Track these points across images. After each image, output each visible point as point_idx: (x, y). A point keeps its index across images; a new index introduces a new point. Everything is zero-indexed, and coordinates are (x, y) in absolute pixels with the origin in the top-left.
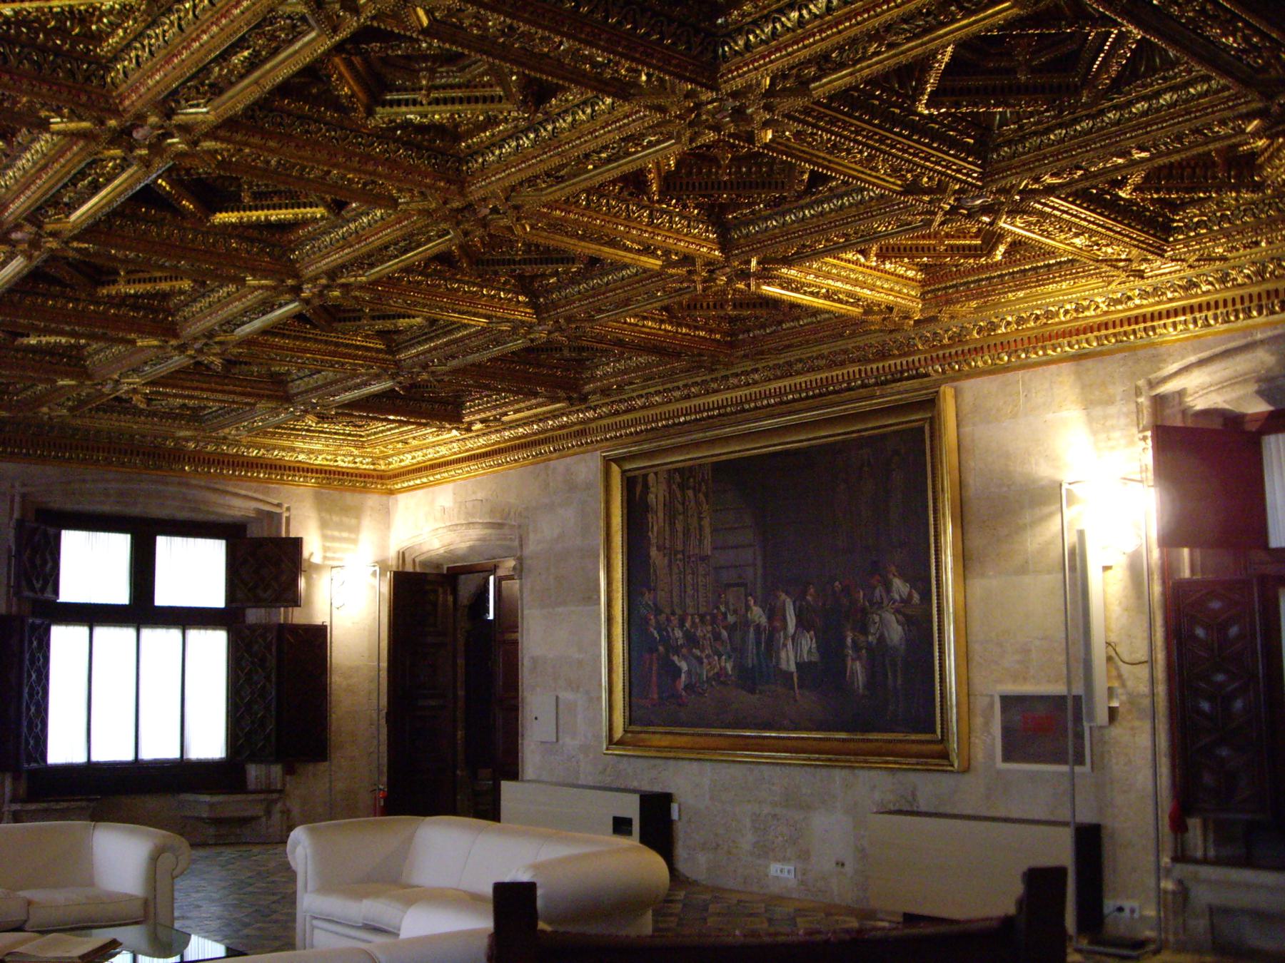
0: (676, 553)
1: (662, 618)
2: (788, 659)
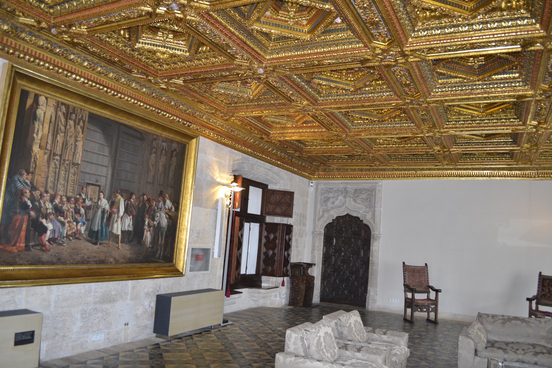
0: (55, 155)
1: (37, 194)
2: (117, 228)
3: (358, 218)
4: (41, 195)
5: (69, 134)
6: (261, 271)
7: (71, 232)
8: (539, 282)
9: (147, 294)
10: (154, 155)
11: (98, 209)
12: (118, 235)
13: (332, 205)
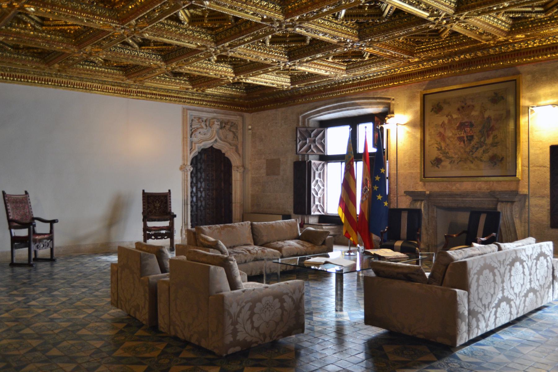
8: (143, 199)
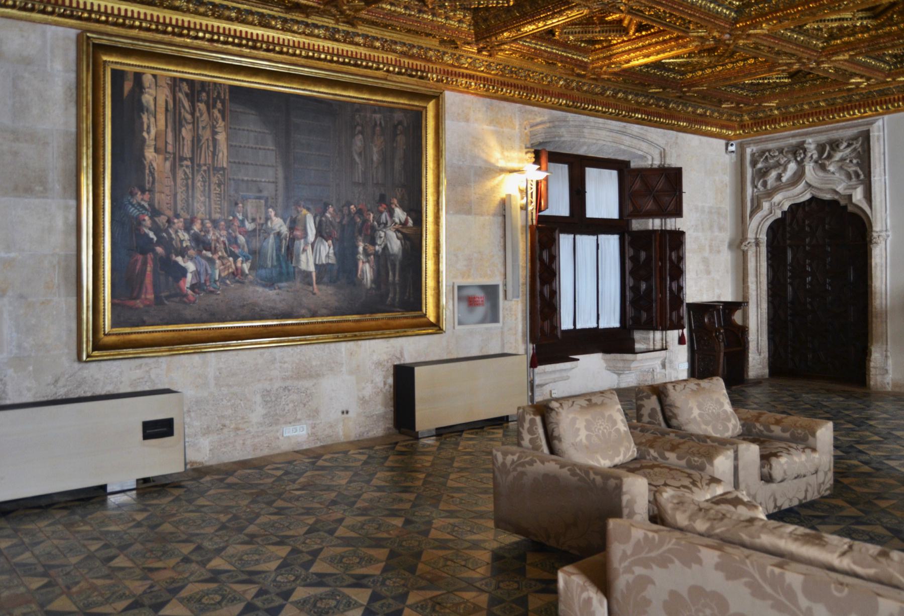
0: (182, 159)
1: (162, 220)
2: (307, 262)
3: (835, 202)
4: (169, 221)
5: (201, 125)
6: (629, 322)
7: (226, 273)
9: (379, 364)
10: (360, 136)
11: (269, 234)
12: (310, 273)
13: (775, 184)
